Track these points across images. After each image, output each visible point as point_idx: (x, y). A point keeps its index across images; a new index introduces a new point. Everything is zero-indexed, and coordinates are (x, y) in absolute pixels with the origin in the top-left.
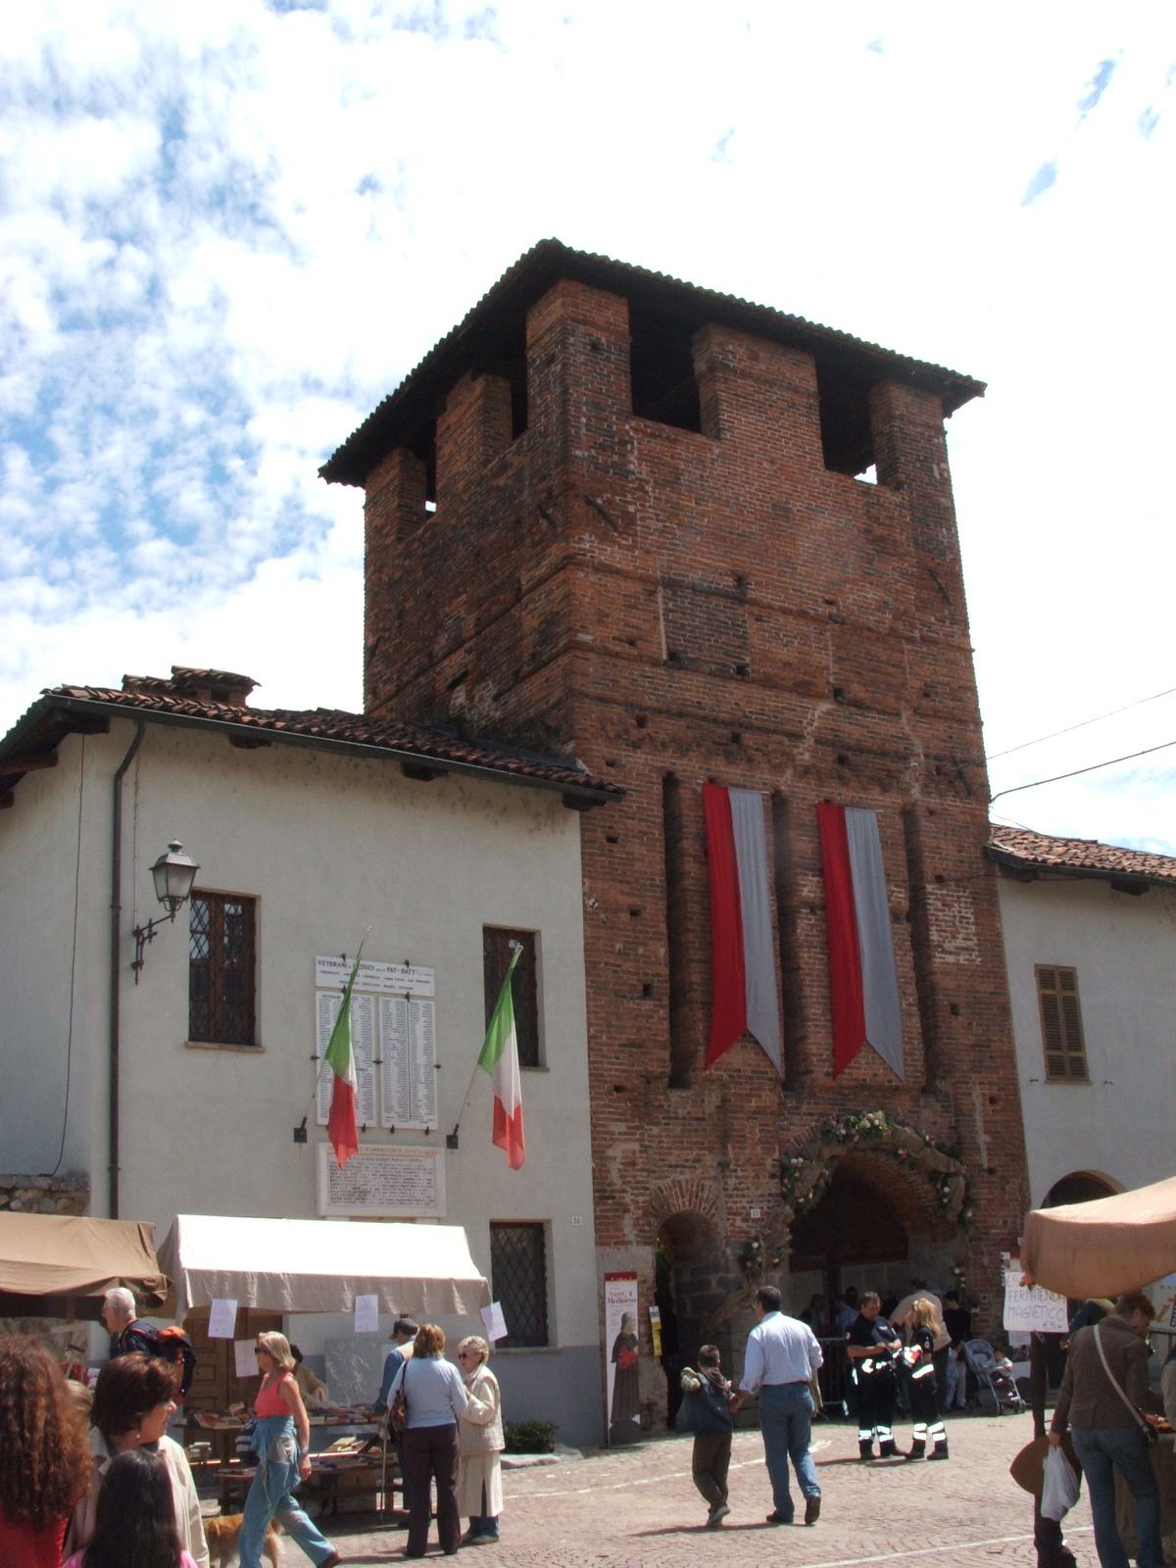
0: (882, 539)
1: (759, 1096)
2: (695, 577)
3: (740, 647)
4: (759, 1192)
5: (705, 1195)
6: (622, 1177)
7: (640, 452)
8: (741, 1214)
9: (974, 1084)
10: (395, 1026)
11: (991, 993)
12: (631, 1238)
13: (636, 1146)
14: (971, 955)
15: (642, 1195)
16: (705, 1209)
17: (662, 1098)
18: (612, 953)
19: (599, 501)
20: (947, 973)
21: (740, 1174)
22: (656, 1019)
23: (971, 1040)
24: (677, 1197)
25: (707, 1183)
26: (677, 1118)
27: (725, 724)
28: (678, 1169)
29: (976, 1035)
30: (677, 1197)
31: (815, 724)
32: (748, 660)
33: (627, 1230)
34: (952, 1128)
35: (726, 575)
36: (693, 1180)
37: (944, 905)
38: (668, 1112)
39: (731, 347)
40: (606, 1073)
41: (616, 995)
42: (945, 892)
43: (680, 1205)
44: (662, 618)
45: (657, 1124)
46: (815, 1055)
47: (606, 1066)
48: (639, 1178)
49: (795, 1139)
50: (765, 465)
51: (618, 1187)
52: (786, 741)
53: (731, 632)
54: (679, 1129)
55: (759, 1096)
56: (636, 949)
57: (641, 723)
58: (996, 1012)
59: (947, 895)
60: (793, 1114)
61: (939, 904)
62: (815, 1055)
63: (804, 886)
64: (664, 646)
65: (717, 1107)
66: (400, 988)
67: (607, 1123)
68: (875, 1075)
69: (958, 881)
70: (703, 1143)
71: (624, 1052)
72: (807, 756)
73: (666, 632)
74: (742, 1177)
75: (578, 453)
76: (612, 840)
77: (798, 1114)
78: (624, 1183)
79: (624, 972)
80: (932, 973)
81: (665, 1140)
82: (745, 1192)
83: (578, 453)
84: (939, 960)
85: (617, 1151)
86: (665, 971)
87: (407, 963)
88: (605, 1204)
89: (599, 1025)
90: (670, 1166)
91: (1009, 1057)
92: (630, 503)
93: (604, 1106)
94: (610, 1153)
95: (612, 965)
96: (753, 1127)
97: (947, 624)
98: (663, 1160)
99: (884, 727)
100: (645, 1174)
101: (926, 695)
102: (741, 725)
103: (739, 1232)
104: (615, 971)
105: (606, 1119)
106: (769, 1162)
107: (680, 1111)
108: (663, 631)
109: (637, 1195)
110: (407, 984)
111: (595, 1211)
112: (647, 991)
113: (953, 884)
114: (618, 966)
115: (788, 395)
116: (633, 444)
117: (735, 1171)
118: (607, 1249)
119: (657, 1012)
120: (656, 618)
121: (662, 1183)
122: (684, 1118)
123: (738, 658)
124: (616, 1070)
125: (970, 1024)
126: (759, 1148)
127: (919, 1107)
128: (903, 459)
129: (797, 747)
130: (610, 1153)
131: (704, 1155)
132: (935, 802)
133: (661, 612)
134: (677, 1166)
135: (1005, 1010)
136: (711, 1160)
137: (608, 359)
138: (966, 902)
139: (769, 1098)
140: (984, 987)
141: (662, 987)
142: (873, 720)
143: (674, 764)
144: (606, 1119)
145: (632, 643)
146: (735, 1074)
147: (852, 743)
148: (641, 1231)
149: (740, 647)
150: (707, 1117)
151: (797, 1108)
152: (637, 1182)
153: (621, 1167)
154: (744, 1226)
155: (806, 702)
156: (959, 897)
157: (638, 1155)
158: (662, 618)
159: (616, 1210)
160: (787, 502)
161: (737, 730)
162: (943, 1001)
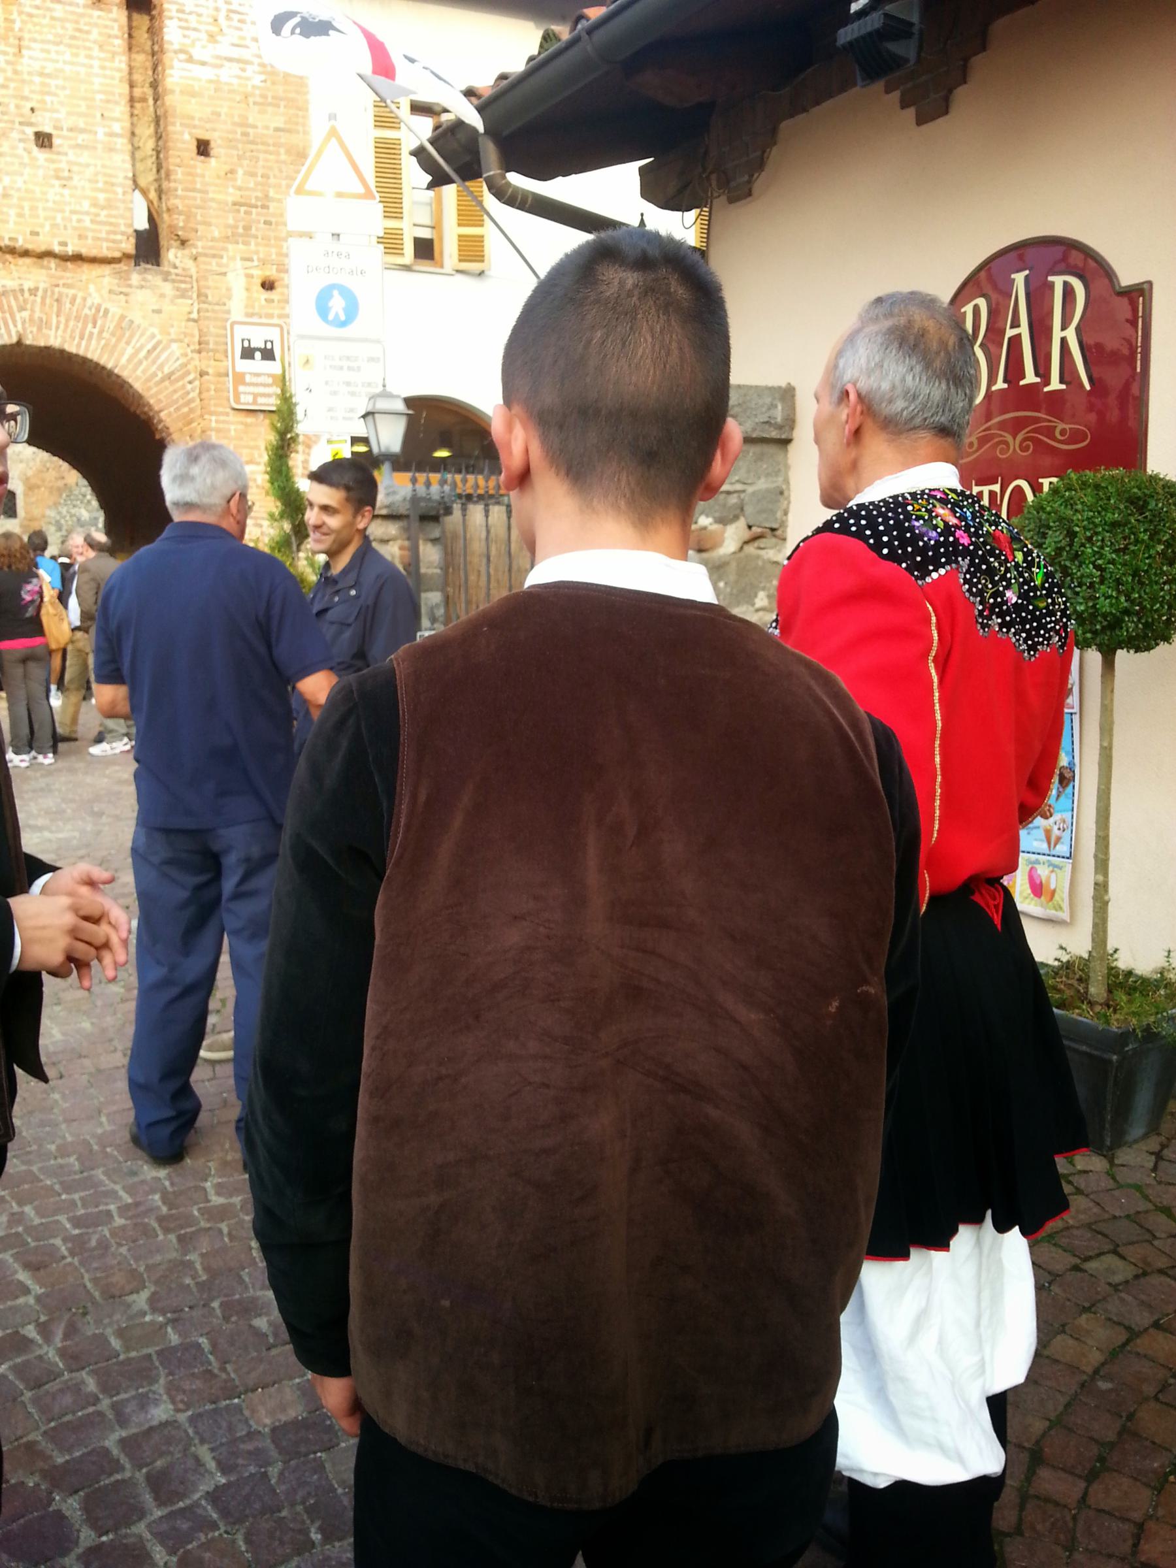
9: (233, 259)
11: (277, 129)
20: (193, 94)
23: (232, 195)
29: (240, 189)
34: (195, 321)
58: (283, 157)
68: (35, 234)
84: (176, 75)
125: (232, 172)
127: (130, 286)
140: (267, 121)
162: (182, 140)
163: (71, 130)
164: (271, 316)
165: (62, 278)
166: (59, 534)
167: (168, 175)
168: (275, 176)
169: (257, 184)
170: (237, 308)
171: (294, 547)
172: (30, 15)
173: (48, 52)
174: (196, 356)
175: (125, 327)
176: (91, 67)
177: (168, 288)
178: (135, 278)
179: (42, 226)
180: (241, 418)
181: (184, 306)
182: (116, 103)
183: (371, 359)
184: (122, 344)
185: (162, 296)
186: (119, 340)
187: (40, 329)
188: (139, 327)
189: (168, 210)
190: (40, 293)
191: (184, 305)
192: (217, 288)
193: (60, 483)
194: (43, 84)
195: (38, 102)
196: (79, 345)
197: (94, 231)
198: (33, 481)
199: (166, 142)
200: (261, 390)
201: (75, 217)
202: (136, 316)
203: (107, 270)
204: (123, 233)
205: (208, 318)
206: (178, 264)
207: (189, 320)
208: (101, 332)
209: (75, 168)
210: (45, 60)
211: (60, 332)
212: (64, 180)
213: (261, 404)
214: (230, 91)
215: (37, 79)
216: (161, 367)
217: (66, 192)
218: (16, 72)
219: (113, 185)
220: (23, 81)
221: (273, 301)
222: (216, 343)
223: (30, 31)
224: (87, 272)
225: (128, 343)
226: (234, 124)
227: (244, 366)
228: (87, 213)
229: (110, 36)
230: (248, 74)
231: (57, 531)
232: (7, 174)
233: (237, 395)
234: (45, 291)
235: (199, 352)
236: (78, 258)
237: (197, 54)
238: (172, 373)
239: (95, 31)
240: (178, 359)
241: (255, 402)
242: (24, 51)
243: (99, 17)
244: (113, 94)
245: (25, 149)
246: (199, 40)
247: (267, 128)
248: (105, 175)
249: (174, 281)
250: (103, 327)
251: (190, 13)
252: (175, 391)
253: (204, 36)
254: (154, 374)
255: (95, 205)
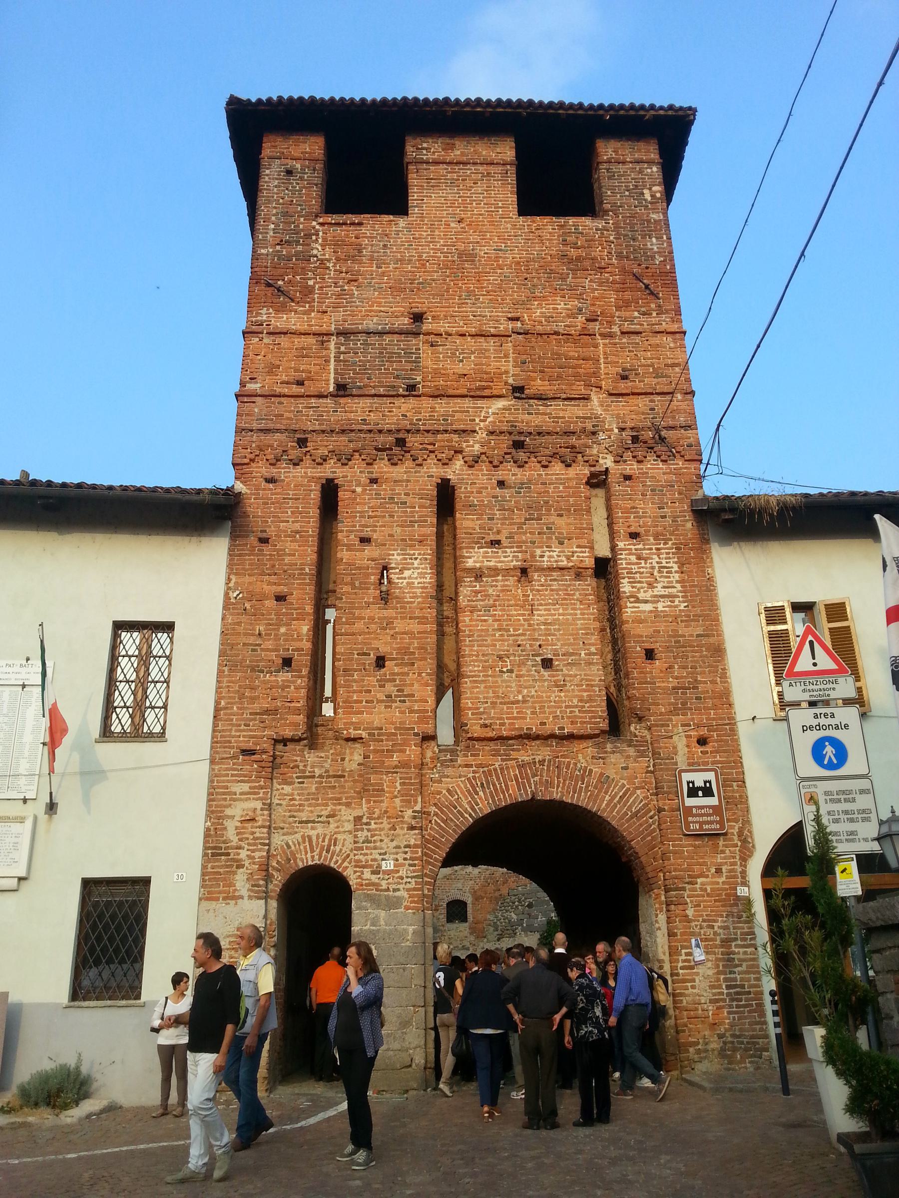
0: (579, 259)
1: (403, 751)
2: (371, 324)
3: (411, 370)
4: (394, 844)
5: (338, 848)
6: (238, 834)
7: (324, 240)
8: (371, 866)
9: (674, 726)
10: (5, 712)
11: (698, 636)
12: (244, 892)
13: (259, 805)
14: (673, 602)
15: (260, 850)
16: (337, 862)
17: (298, 759)
18: (253, 635)
19: (280, 283)
20: (641, 621)
21: (373, 826)
22: (292, 687)
23: (672, 683)
24: (306, 853)
25: (339, 836)
26: (313, 777)
27: (389, 431)
28: (309, 825)
30: (306, 853)
31: (489, 420)
32: (419, 379)
33: (238, 885)
35: (402, 315)
36: (325, 835)
37: (639, 558)
38: (304, 772)
39: (425, 145)
40: (233, 740)
41: (253, 670)
42: (641, 546)
43: (307, 859)
44: (332, 360)
45: (292, 783)
46: (470, 709)
47: (233, 733)
48: (257, 835)
49: (448, 791)
50: (453, 225)
51: (234, 844)
52: (455, 437)
53: (403, 360)
54: (314, 786)
55: (403, 751)
56: (278, 630)
57: (302, 442)
59: (644, 549)
60: (448, 766)
61: (633, 558)
62: (470, 709)
63: (470, 557)
64: (332, 381)
65: (359, 765)
66: (16, 679)
67: (229, 784)
69: (656, 537)
70: (340, 799)
71: (255, 720)
72: (477, 447)
73: (335, 370)
74: (375, 830)
75: (263, 251)
76: (264, 541)
77: (454, 767)
78: (240, 840)
79: (262, 650)
80: (623, 623)
81: (298, 798)
82: (378, 844)
83: (263, 251)
84: (629, 610)
85: (237, 811)
86: (307, 645)
87: (28, 659)
88: (219, 861)
89: (230, 698)
90: (301, 822)
91: (724, 698)
92: (310, 279)
93: (227, 769)
94: (228, 812)
95: (251, 645)
96: (393, 782)
97: (654, 314)
98: (294, 817)
99: (571, 412)
100: (265, 830)
101: (624, 378)
102: (408, 431)
103: (367, 885)
104: (253, 650)
105: (228, 781)
106: (409, 813)
107: (316, 770)
108: (332, 371)
109: (253, 851)
110: (24, 676)
111: (204, 867)
112: (287, 662)
113: (651, 538)
114: (257, 645)
115: (481, 168)
116: (318, 235)
117: (368, 824)
118: (213, 904)
119: (294, 682)
120: (327, 361)
121: (290, 839)
122: (321, 776)
123: (408, 379)
124: (244, 736)
125: (671, 667)
126: (397, 801)
127: (606, 752)
128: (609, 193)
129: (468, 441)
130: (228, 812)
131: (340, 810)
132: (631, 467)
133: (332, 355)
134: (307, 822)
135: (719, 651)
136: (347, 815)
137: (301, 178)
138: (668, 553)
139: (412, 752)
141: (303, 661)
142: (555, 408)
143: (335, 472)
144: (228, 781)
145: (300, 383)
146: (376, 732)
147: (531, 430)
148: (253, 886)
149: (411, 370)
150: (346, 774)
151: (451, 760)
152: (255, 839)
153: (239, 824)
154: (374, 878)
155: (480, 403)
156: (658, 549)
157: (259, 812)
158: (332, 360)
159: (227, 867)
160: (473, 250)
161: (401, 436)
162: (636, 650)
163: (564, 655)
164: (707, 763)
165: (560, 752)
166: (496, 933)
167: (627, 675)
168: (701, 667)
169: (688, 673)
170: (681, 760)
171: (842, 956)
172: (538, 591)
173: (549, 610)
174: (654, 797)
175: (604, 781)
176: (576, 614)
177: (631, 751)
178: (609, 746)
179: (548, 718)
180: (691, 841)
181: (645, 762)
182: (592, 634)
183: (862, 792)
184: (602, 794)
185: (628, 757)
186: (600, 791)
187: (546, 788)
188: (613, 780)
189: (629, 698)
190: (546, 764)
191: (644, 762)
192: (666, 748)
193: (497, 894)
194: (546, 629)
195: (543, 640)
196: (573, 796)
197: (581, 717)
198: (479, 893)
199: (625, 654)
200: (705, 818)
201: (568, 710)
202: (611, 773)
203: (590, 743)
204: (600, 717)
205: (661, 769)
206: (637, 734)
207: (647, 772)
208: (587, 787)
209: (568, 679)
210: (547, 615)
211: (560, 789)
212: (561, 687)
213: (706, 830)
214: (665, 616)
215: (543, 627)
216: (630, 807)
217: (562, 694)
218: (530, 625)
219: (592, 686)
220: (534, 630)
221: (707, 752)
222: (669, 787)
223: (538, 600)
224: (577, 746)
225: (606, 793)
226: (669, 636)
227: (690, 802)
228: (576, 706)
229: (586, 595)
230: (677, 603)
231: (494, 931)
232: (526, 688)
233: (687, 824)
234: (550, 761)
235: (657, 794)
236: (571, 737)
237: (641, 595)
238: (638, 811)
239: (577, 593)
240: (642, 801)
241: (701, 829)
242: (534, 612)
243: (579, 585)
244: (589, 629)
245: (536, 671)
246: (642, 588)
247: (692, 635)
248: (587, 680)
249: (636, 746)
250: (588, 782)
251: (636, 573)
252: (641, 825)
253: (645, 585)
254: (626, 814)
255: (581, 701)
